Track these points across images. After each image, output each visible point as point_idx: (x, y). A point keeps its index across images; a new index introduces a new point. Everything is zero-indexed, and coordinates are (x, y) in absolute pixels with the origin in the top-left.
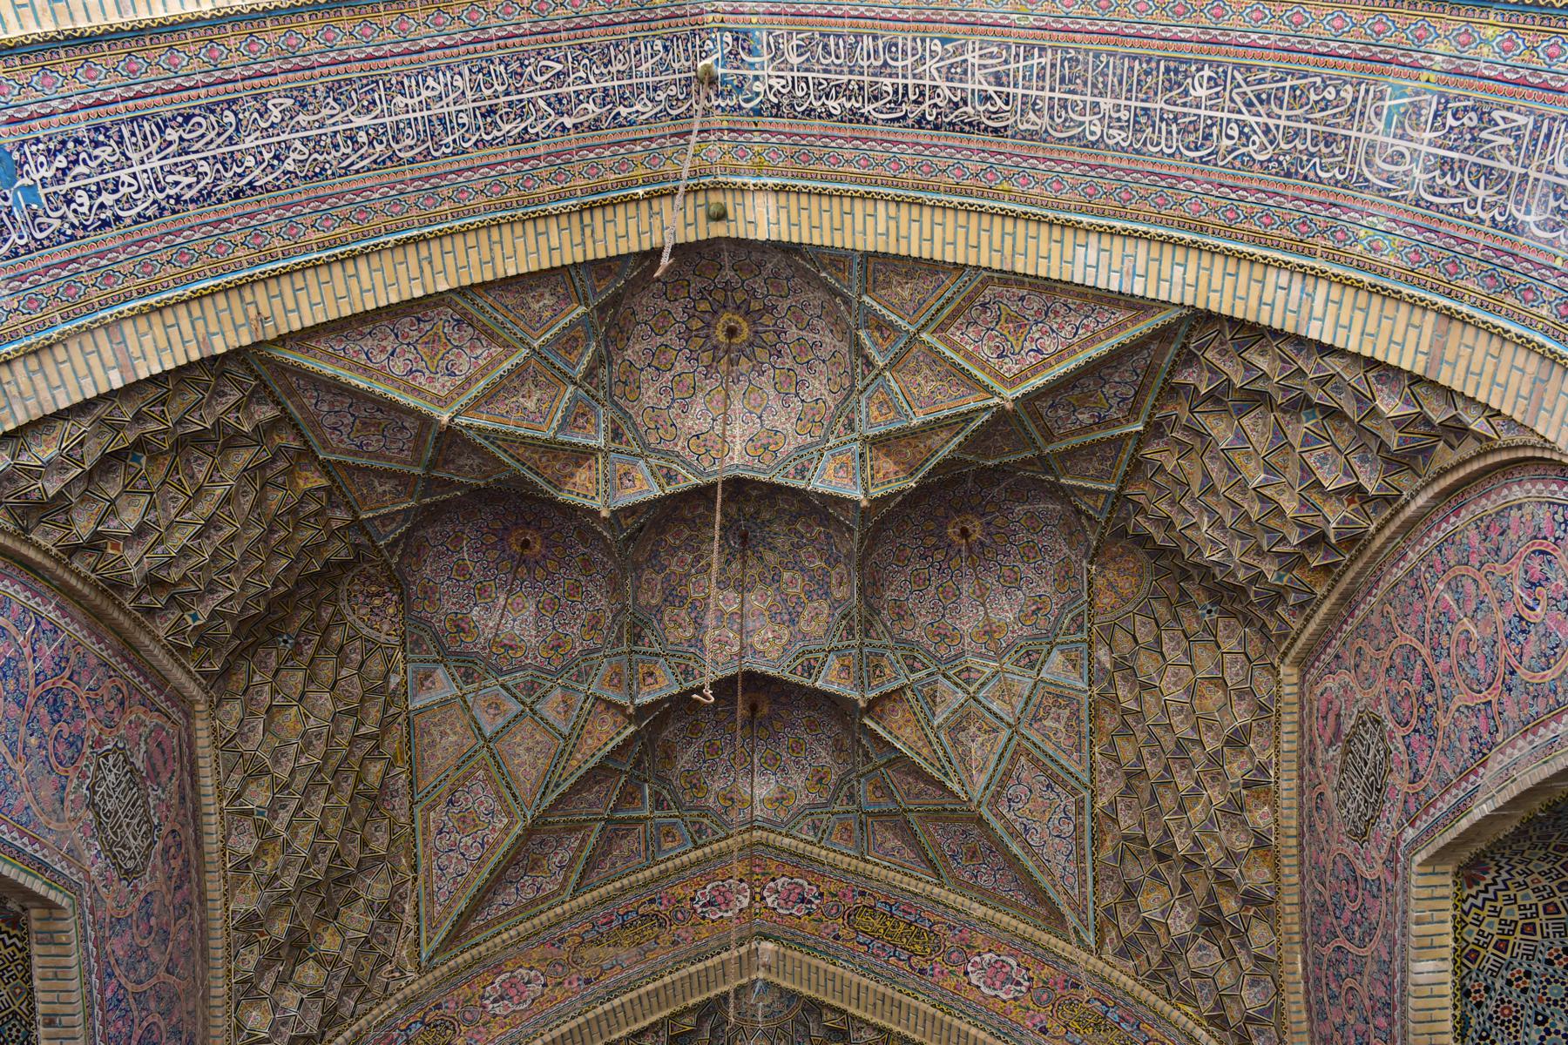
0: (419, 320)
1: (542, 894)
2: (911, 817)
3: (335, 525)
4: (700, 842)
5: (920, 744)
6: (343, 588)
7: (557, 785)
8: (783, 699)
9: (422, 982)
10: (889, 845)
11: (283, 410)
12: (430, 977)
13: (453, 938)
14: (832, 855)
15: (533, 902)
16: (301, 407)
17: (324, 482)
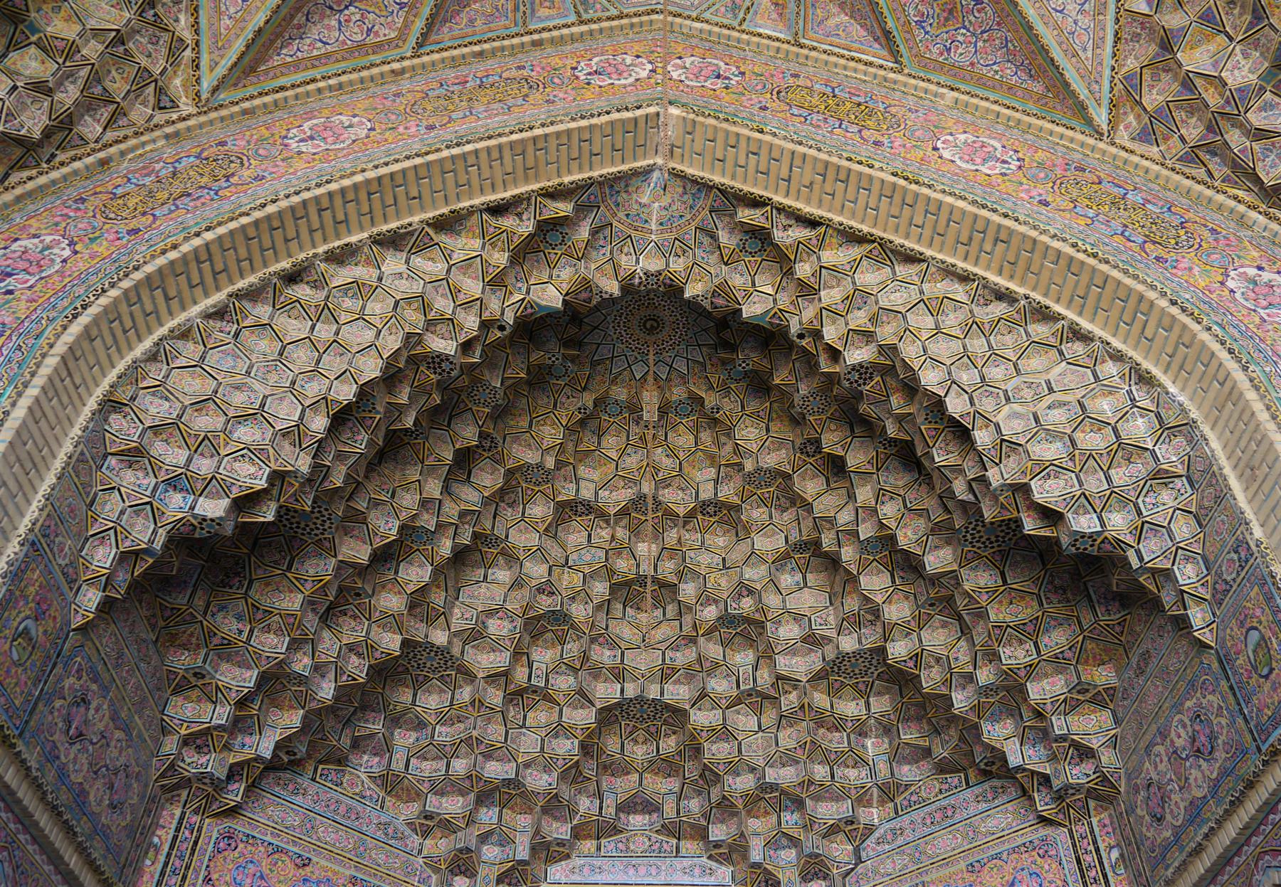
1: (372, 39)
4: (585, 16)
9: (203, 119)
10: (832, 22)
12: (213, 115)
13: (249, 65)
14: (756, 39)
15: (360, 47)
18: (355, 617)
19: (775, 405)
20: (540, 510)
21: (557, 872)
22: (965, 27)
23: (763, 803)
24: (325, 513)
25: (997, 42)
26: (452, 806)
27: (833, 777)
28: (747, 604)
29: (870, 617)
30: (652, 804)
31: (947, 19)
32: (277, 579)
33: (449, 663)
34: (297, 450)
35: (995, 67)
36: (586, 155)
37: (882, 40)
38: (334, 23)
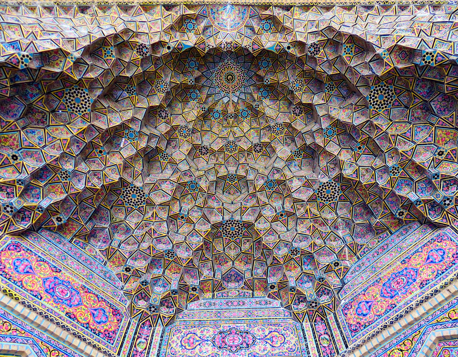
18: (99, 164)
19: (281, 102)
20: (186, 148)
21: (193, 306)
23: (292, 262)
24: (87, 97)
26: (141, 264)
27: (325, 243)
28: (277, 176)
29: (332, 166)
30: (239, 275)
32: (62, 127)
33: (143, 199)
34: (74, 50)
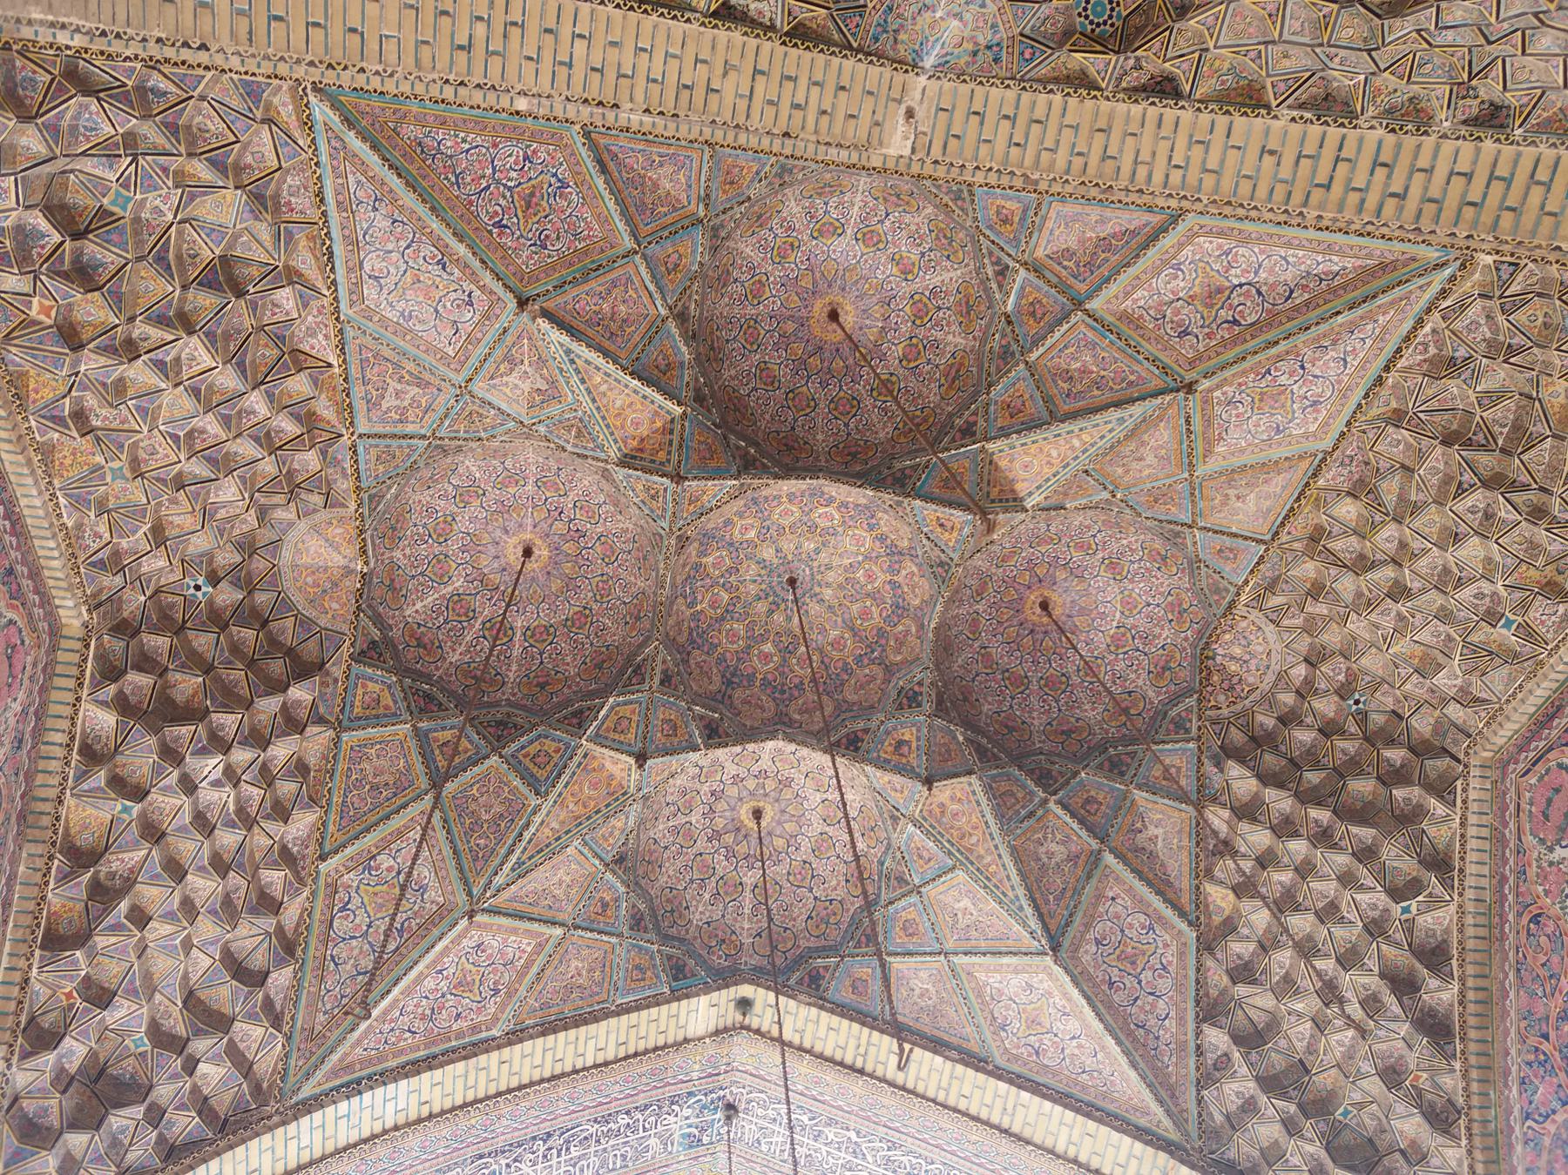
0: (1037, 1053)
1: (1226, 244)
2: (628, 243)
3: (1226, 814)
5: (604, 388)
6: (1265, 686)
7: (1121, 420)
8: (790, 327)
11: (1198, 1035)
16: (1181, 1021)
17: (1210, 888)
22: (510, 189)
25: (468, 179)
31: (532, 194)
35: (467, 146)
36: (1022, 121)
37: (606, 157)
38: (1263, 275)
